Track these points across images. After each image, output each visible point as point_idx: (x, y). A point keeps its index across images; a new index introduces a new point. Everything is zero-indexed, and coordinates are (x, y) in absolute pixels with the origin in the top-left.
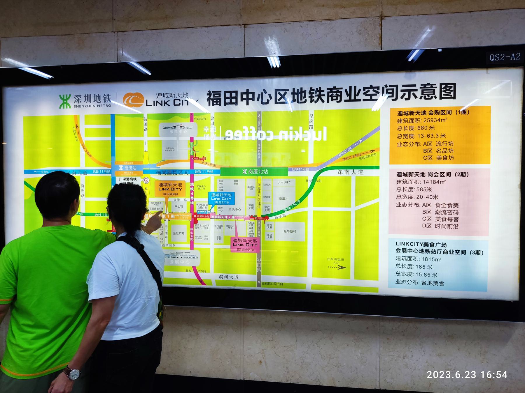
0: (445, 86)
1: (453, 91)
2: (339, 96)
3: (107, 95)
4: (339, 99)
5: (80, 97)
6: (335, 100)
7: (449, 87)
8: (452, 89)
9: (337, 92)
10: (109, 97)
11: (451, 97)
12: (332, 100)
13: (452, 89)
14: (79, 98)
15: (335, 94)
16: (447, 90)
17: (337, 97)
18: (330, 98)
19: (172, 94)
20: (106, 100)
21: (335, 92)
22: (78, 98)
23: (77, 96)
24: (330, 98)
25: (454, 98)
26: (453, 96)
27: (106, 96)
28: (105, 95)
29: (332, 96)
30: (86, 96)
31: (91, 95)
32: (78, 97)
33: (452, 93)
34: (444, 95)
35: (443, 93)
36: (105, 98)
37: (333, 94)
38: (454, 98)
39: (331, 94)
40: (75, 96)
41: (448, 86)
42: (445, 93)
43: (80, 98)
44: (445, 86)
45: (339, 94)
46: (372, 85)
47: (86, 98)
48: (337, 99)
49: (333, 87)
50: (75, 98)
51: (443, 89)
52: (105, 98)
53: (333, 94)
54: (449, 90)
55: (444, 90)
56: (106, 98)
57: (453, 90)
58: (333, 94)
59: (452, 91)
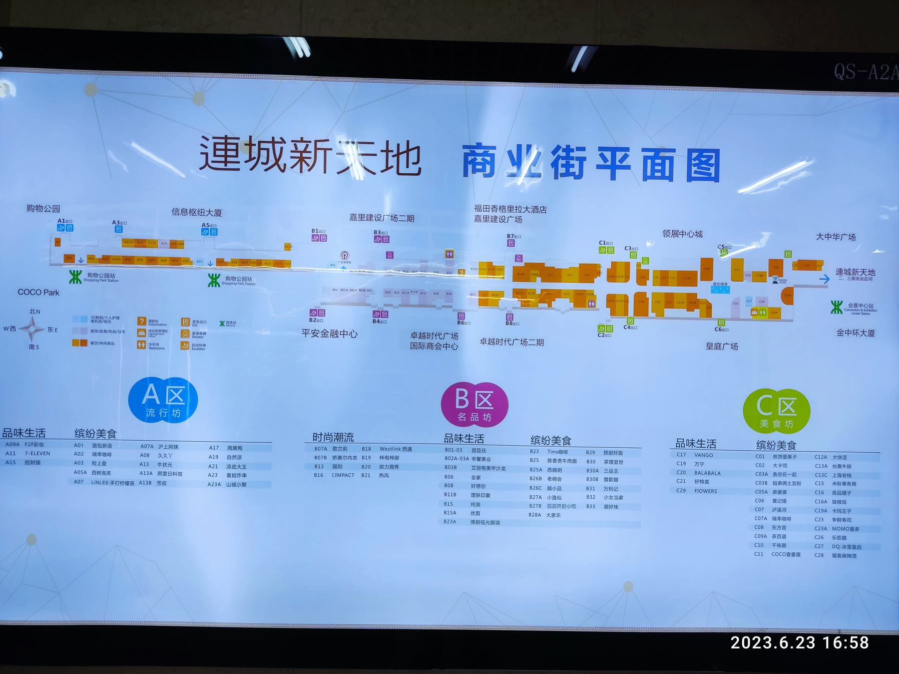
0: (697, 154)
1: (714, 166)
2: (488, 163)
4: (488, 171)
6: (479, 170)
7: (705, 157)
8: (712, 161)
9: (486, 154)
11: (709, 178)
12: (475, 171)
13: (712, 161)
15: (479, 159)
16: (701, 162)
17: (483, 164)
18: (470, 167)
21: (479, 155)
24: (470, 167)
25: (716, 179)
26: (713, 175)
29: (474, 163)
33: (712, 170)
34: (696, 172)
35: (694, 169)
37: (477, 159)
38: (716, 179)
39: (473, 157)
41: (704, 154)
42: (697, 168)
44: (697, 154)
45: (488, 158)
46: (570, 146)
48: (483, 170)
49: (476, 145)
51: (695, 160)
53: (477, 159)
54: (706, 163)
55: (697, 162)
57: (714, 163)
58: (475, 159)
59: (712, 165)
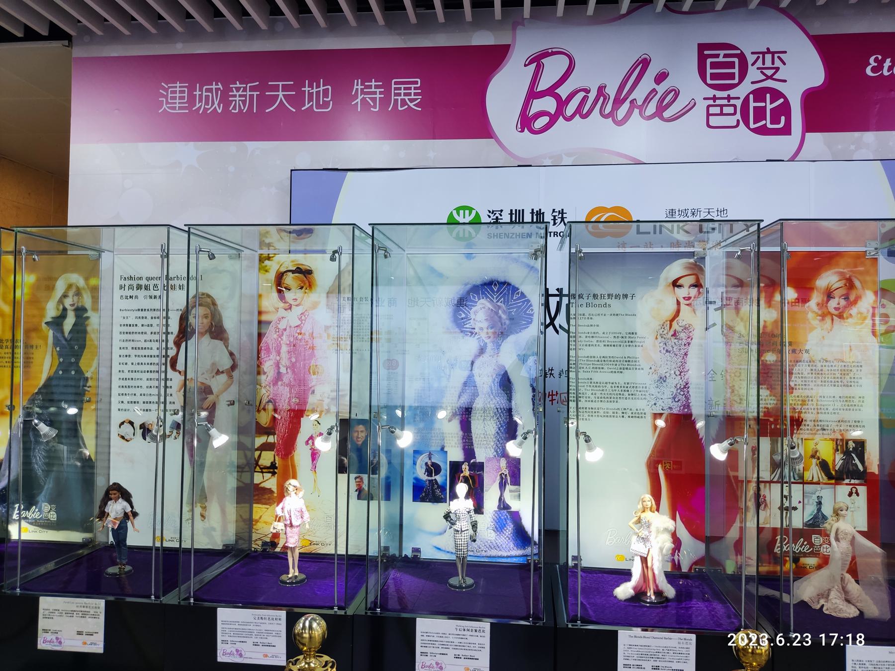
3: (559, 211)
5: (501, 215)
10: (562, 216)
14: (497, 217)
19: (696, 211)
20: (556, 221)
22: (495, 217)
23: (493, 211)
27: (557, 214)
28: (554, 211)
30: (514, 212)
31: (523, 210)
32: (495, 214)
36: (555, 217)
40: (490, 212)
43: (500, 217)
47: (514, 216)
50: (489, 217)
52: (555, 217)
56: (557, 218)
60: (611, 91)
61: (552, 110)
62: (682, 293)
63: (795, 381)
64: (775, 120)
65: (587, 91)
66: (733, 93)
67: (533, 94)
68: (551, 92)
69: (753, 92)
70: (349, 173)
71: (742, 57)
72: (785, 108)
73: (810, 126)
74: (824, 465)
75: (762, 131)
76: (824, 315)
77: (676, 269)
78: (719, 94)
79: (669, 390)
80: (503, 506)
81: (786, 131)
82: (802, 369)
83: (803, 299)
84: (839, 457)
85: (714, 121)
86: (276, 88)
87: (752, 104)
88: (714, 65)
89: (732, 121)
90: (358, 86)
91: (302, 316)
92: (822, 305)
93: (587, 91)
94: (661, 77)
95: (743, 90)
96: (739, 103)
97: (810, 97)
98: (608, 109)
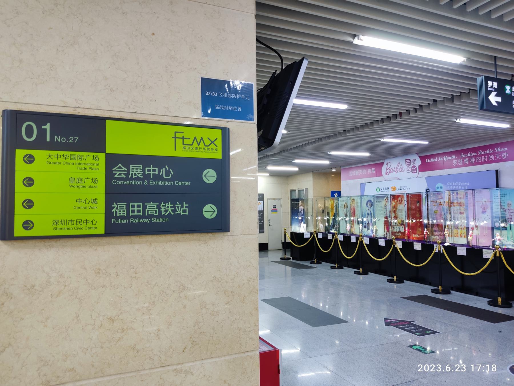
60: (396, 168)
61: (389, 172)
62: (386, 201)
63: (397, 212)
64: (415, 171)
65: (393, 168)
66: (410, 167)
67: (387, 169)
68: (389, 169)
69: (412, 166)
70: (366, 184)
71: (410, 161)
72: (416, 169)
73: (420, 171)
74: (400, 223)
75: (413, 173)
76: (399, 203)
77: (385, 198)
78: (409, 167)
79: (385, 213)
80: (371, 229)
81: (416, 172)
82: (397, 211)
83: (397, 201)
84: (401, 222)
85: (408, 172)
86: (360, 171)
87: (412, 168)
88: (408, 163)
89: (409, 171)
90: (368, 170)
91: (354, 205)
92: (399, 202)
93: (393, 168)
94: (401, 165)
95: (411, 166)
96: (410, 168)
97: (420, 166)
98: (395, 171)
